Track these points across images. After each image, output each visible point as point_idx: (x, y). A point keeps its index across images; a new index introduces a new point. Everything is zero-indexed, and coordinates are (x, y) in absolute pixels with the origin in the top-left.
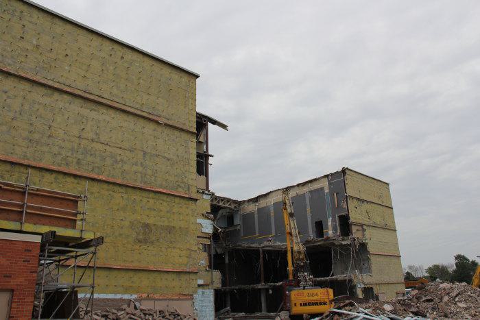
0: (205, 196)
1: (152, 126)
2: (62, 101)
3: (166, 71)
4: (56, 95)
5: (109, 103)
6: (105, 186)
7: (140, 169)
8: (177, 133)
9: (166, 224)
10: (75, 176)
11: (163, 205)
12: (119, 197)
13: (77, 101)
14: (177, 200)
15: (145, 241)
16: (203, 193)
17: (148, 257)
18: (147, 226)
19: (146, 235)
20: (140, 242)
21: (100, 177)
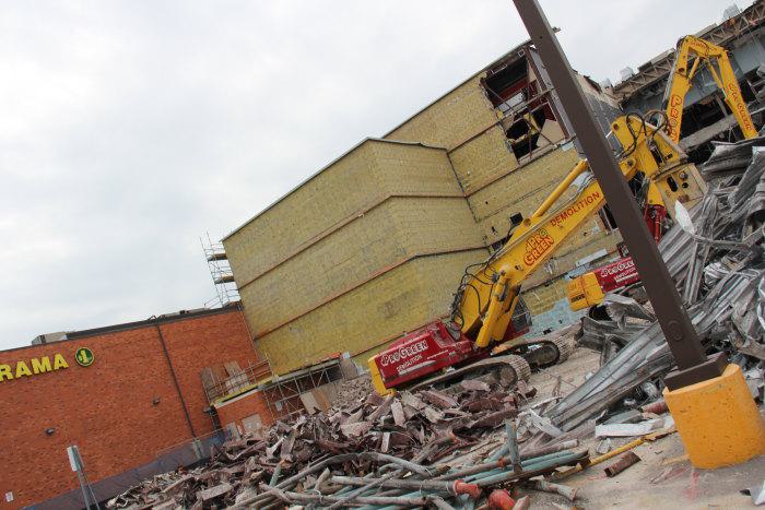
0: (564, 149)
1: (358, 223)
2: (307, 257)
3: (345, 165)
4: (304, 255)
5: (328, 232)
6: (353, 293)
7: (365, 264)
8: (376, 211)
9: (400, 293)
10: (335, 299)
11: (392, 280)
12: (363, 294)
13: (313, 249)
14: (400, 269)
15: (391, 316)
16: (559, 146)
18: (387, 304)
19: (390, 310)
20: (388, 318)
21: (348, 289)
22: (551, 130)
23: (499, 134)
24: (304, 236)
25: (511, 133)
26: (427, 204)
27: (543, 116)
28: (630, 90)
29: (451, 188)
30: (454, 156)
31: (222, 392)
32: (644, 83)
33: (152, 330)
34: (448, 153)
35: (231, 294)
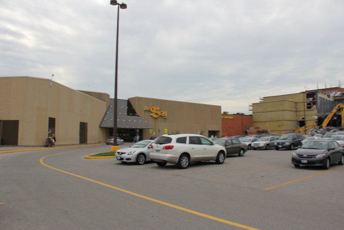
17: (279, 129)
19: (279, 126)
22: (314, 106)
23: (306, 104)
24: (269, 109)
25: (308, 104)
26: (290, 112)
27: (314, 104)
28: (337, 98)
29: (294, 109)
30: (298, 104)
31: (248, 129)
32: (340, 98)
33: (241, 116)
34: (296, 103)
35: (251, 113)
